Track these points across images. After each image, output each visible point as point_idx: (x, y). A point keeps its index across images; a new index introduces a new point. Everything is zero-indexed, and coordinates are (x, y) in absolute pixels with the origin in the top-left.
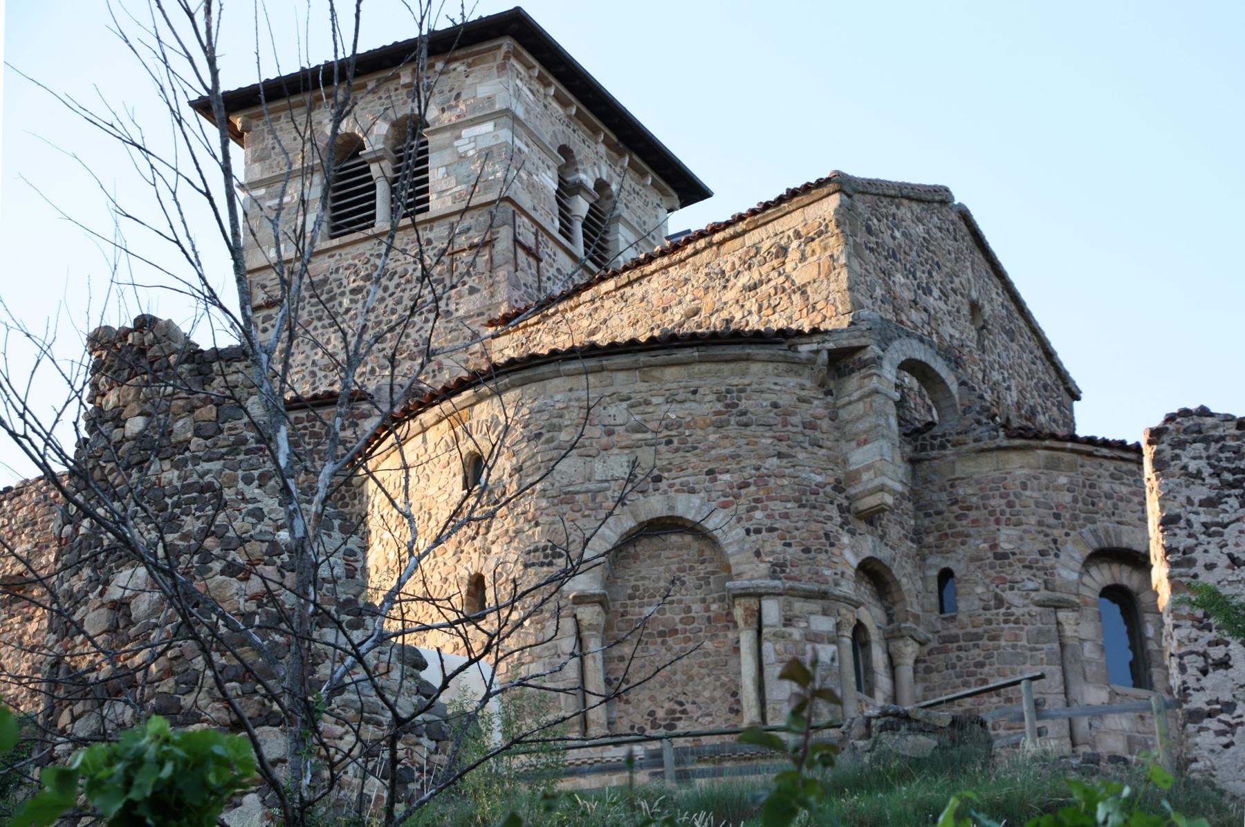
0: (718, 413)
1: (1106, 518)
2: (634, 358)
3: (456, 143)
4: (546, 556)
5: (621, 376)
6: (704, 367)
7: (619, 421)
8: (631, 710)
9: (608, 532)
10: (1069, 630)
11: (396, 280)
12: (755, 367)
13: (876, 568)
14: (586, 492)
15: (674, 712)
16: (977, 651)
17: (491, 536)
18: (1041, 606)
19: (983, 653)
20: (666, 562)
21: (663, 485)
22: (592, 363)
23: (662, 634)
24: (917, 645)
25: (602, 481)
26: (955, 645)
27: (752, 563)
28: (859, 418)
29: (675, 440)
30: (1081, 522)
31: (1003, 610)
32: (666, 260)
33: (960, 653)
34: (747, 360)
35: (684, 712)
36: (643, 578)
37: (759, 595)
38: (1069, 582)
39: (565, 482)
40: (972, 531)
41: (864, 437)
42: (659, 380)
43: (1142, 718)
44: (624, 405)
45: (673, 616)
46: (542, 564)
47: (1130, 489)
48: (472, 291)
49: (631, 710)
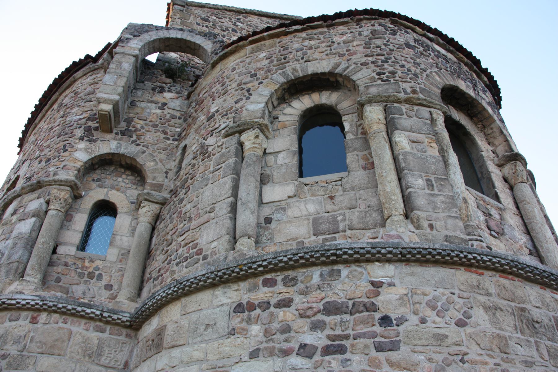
1: (295, 62)
10: (248, 145)
13: (129, 162)
24: (157, 206)
30: (274, 71)
38: (254, 111)
43: (331, 198)
47: (318, 41)
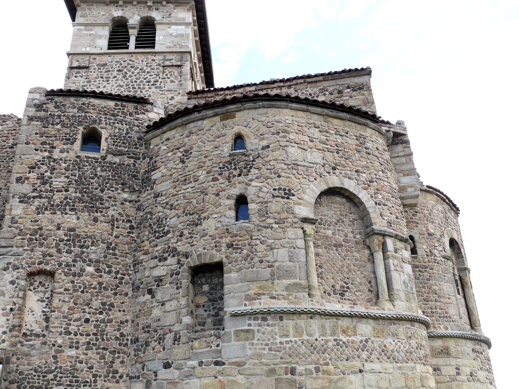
0: (357, 145)
2: (322, 110)
3: (168, 29)
4: (285, 194)
5: (315, 116)
6: (350, 123)
7: (315, 137)
8: (324, 283)
9: (315, 188)
11: (138, 70)
12: (369, 130)
14: (304, 166)
15: (343, 287)
16: (426, 274)
17: (250, 177)
18: (444, 258)
19: (429, 275)
20: (335, 209)
21: (337, 171)
22: (304, 107)
23: (335, 245)
25: (311, 163)
26: (418, 269)
27: (380, 219)
28: (403, 164)
29: (341, 152)
31: (433, 257)
32: (282, 84)
33: (420, 273)
34: (366, 125)
35: (348, 288)
36: (325, 215)
37: (384, 236)
39: (293, 158)
40: (419, 222)
41: (406, 173)
42: (332, 123)
44: (317, 130)
45: (340, 238)
46: (283, 198)
48: (172, 81)
49: (324, 283)
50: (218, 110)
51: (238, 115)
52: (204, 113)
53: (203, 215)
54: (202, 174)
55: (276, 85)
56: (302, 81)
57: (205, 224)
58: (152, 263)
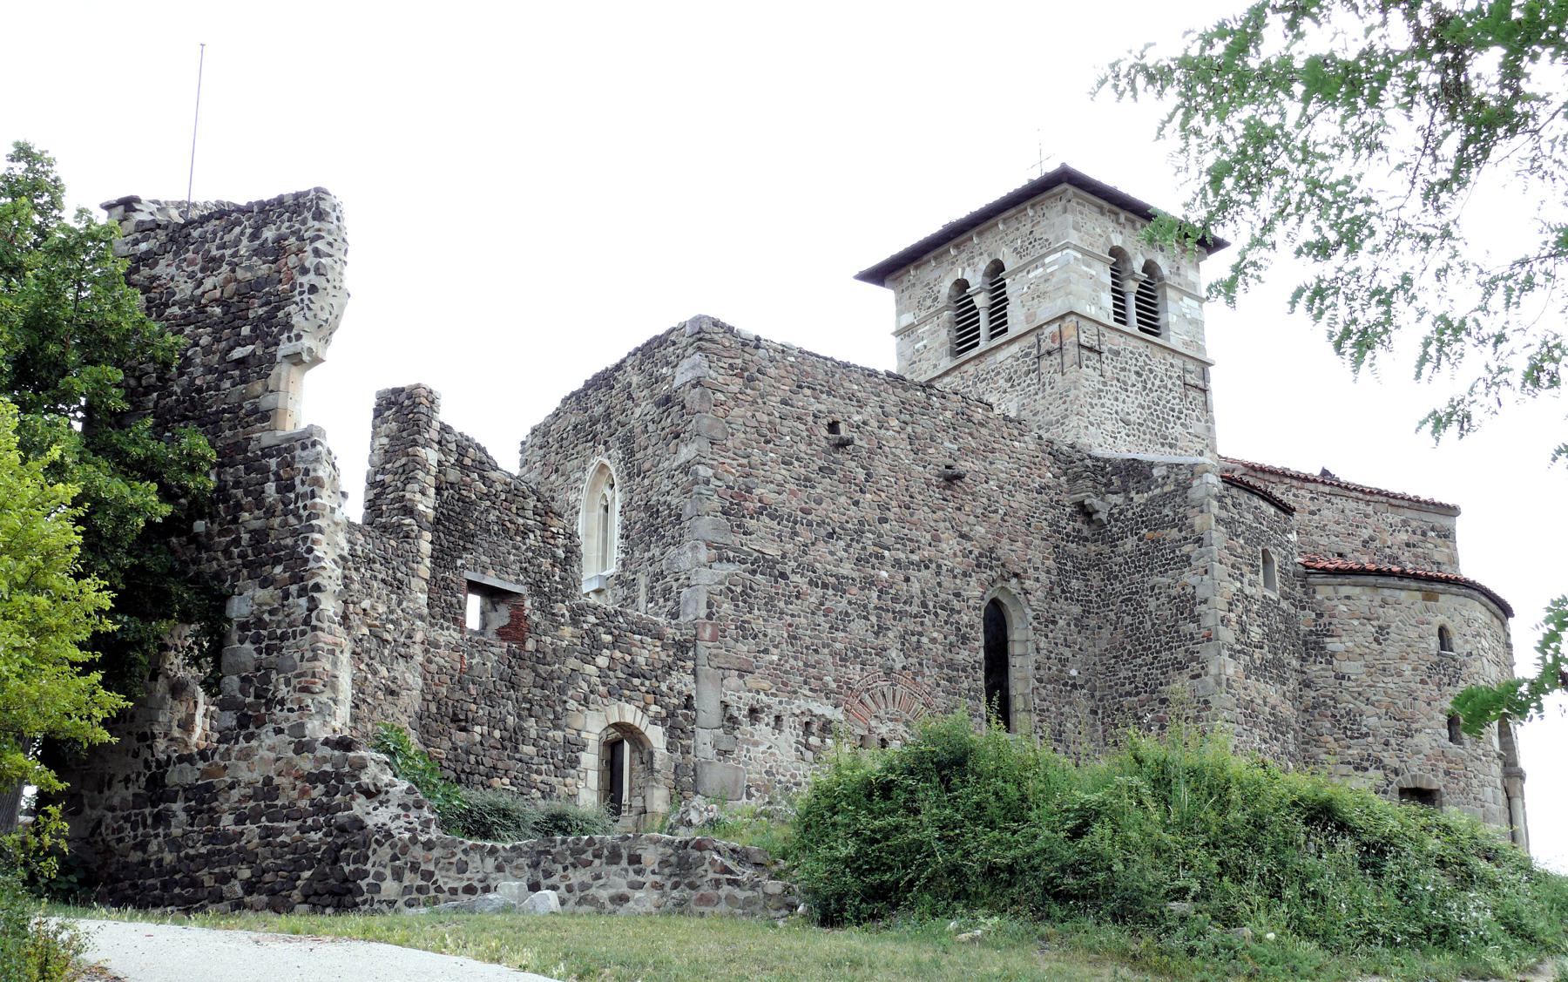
50: (1423, 585)
51: (1442, 598)
52: (1405, 582)
53: (1414, 726)
54: (1407, 669)
55: (1354, 494)
56: (1384, 499)
57: (1418, 738)
58: (1345, 769)
